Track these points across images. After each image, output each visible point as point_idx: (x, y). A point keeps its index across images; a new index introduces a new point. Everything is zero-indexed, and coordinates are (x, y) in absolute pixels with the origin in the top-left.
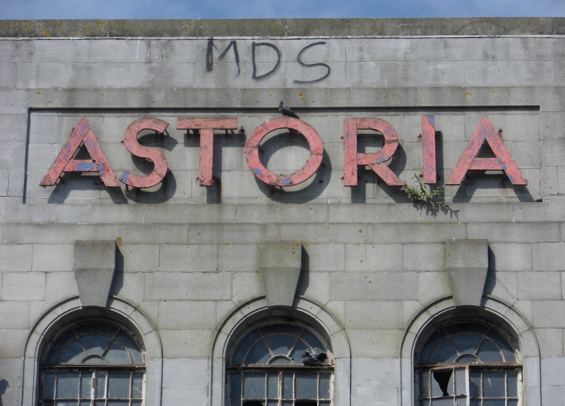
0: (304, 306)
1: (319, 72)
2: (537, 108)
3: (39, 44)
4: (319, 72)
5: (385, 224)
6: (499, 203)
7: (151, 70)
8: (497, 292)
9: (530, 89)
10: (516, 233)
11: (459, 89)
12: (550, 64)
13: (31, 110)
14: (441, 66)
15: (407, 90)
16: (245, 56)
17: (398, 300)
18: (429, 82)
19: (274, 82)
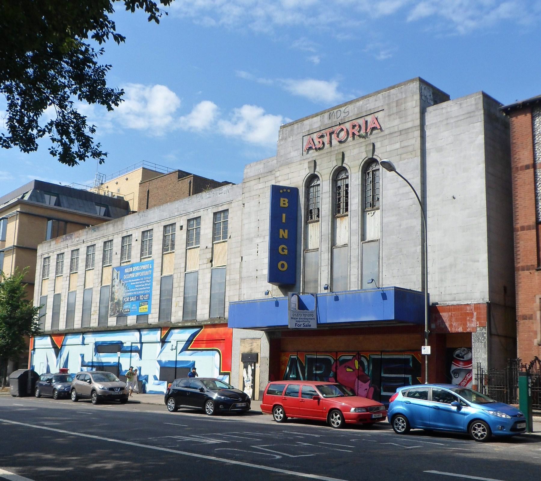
0: (344, 165)
1: (347, 114)
2: (383, 110)
3: (304, 122)
4: (347, 114)
5: (357, 144)
6: (377, 133)
7: (321, 122)
8: (375, 153)
9: (382, 106)
10: (379, 139)
11: (370, 110)
12: (387, 98)
13: (303, 136)
14: (367, 105)
15: (361, 113)
16: (335, 114)
17: (359, 160)
18: (365, 110)
19: (340, 118)
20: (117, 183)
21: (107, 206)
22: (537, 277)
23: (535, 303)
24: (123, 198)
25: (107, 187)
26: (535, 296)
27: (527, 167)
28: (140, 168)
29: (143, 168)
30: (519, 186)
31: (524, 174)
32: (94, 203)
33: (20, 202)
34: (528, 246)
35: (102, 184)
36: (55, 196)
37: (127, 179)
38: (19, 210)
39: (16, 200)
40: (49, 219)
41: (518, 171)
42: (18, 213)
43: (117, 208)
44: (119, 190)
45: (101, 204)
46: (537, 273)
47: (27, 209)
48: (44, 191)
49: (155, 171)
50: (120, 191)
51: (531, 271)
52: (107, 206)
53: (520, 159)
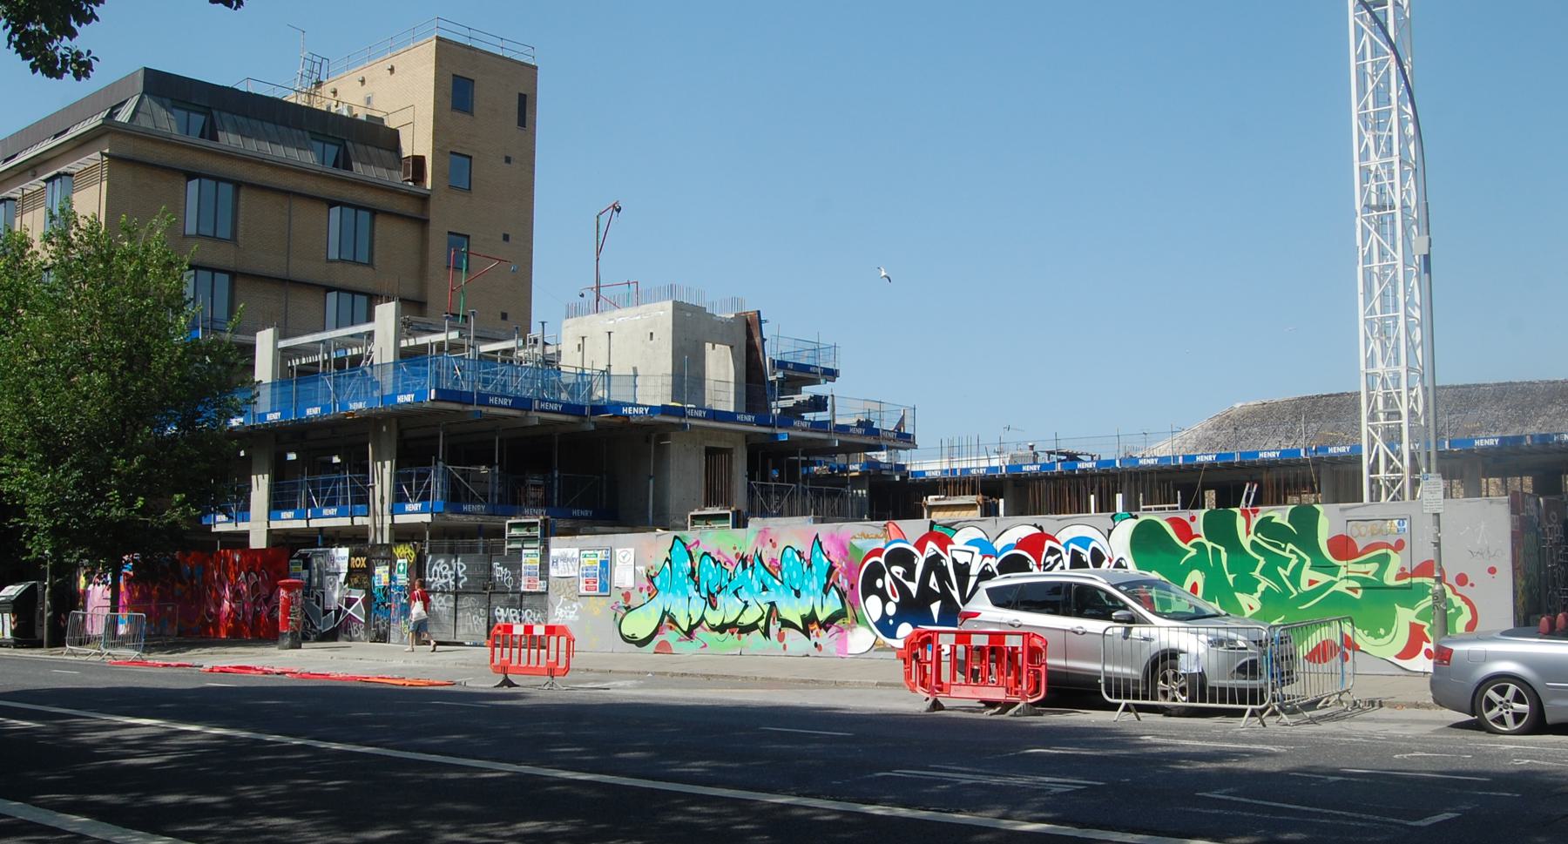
20: (363, 82)
21: (344, 141)
24: (382, 120)
25: (335, 93)
28: (429, 39)
29: (438, 38)
32: (307, 135)
33: (108, 128)
35: (319, 84)
37: (392, 70)
38: (107, 151)
39: (95, 121)
40: (190, 176)
42: (105, 158)
43: (369, 148)
44: (369, 100)
45: (325, 135)
47: (129, 148)
48: (172, 99)
49: (470, 48)
50: (374, 103)
52: (344, 141)
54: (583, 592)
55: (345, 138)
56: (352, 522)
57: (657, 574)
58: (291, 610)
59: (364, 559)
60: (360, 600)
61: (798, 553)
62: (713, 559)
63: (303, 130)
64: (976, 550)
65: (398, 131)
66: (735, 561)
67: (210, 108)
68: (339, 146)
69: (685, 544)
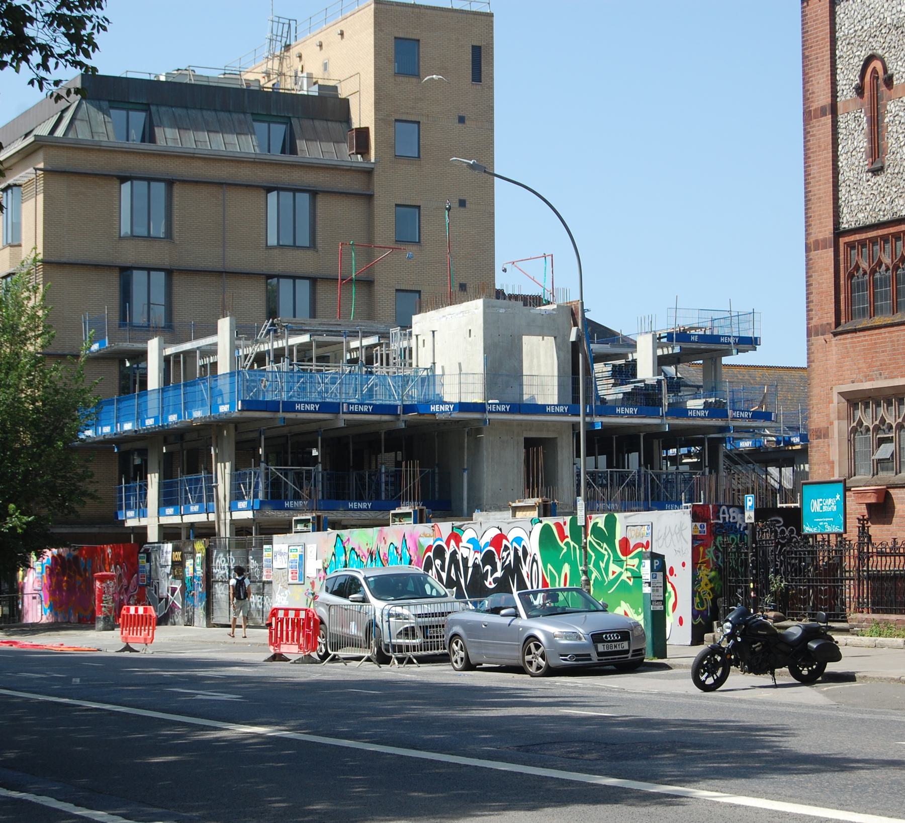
21: (289, 118)
22: (834, 349)
23: (832, 403)
24: (335, 88)
26: (831, 389)
27: (822, 112)
30: (812, 152)
31: (819, 126)
32: (249, 118)
34: (823, 283)
35: (287, 47)
36: (142, 110)
37: (342, 34)
38: (41, 166)
40: (123, 179)
41: (811, 120)
42: (39, 172)
43: (317, 123)
44: (325, 66)
46: (834, 340)
47: (63, 160)
48: (109, 101)
51: (826, 336)
53: (813, 93)
54: (291, 581)
55: (290, 115)
56: (208, 518)
57: (328, 566)
58: (103, 598)
59: (180, 553)
60: (178, 590)
61: (396, 548)
62: (356, 553)
63: (244, 113)
64: (471, 546)
65: (348, 100)
66: (367, 554)
67: (148, 105)
68: (286, 123)
69: (342, 541)
